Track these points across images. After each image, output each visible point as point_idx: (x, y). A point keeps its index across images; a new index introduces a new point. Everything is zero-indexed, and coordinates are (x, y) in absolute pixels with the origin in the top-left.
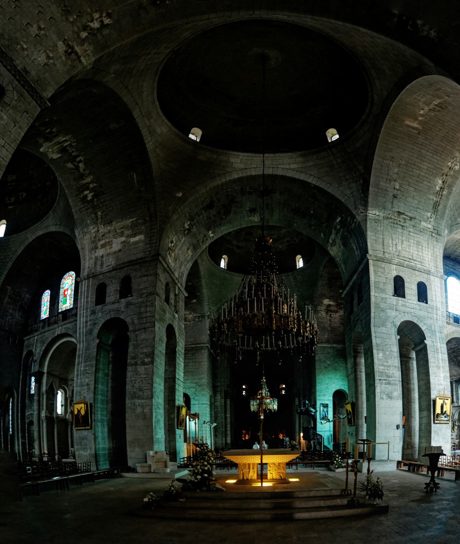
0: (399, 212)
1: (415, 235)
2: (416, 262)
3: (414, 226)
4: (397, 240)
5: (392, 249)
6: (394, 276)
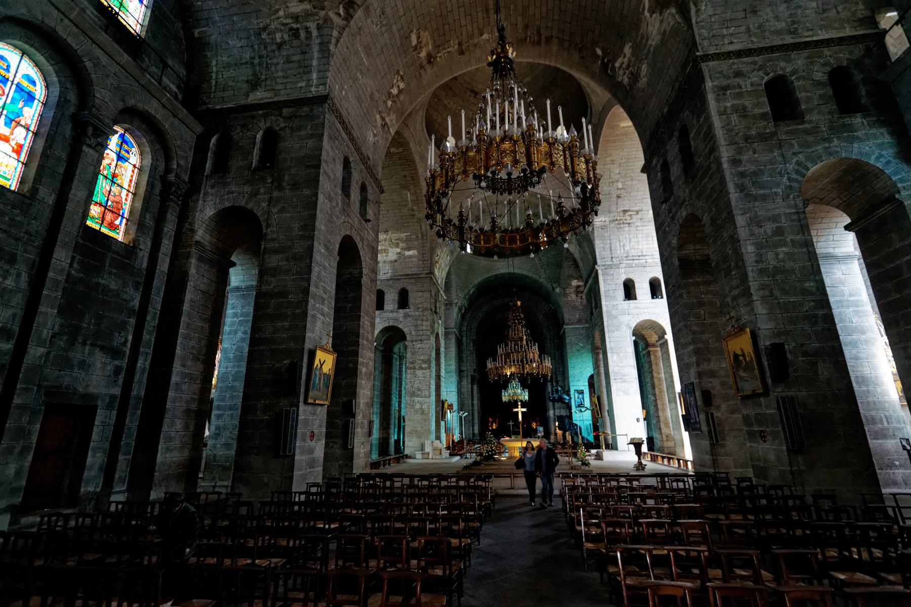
1: (644, 228)
2: (646, 257)
3: (641, 219)
4: (624, 241)
5: (619, 252)
6: (623, 280)
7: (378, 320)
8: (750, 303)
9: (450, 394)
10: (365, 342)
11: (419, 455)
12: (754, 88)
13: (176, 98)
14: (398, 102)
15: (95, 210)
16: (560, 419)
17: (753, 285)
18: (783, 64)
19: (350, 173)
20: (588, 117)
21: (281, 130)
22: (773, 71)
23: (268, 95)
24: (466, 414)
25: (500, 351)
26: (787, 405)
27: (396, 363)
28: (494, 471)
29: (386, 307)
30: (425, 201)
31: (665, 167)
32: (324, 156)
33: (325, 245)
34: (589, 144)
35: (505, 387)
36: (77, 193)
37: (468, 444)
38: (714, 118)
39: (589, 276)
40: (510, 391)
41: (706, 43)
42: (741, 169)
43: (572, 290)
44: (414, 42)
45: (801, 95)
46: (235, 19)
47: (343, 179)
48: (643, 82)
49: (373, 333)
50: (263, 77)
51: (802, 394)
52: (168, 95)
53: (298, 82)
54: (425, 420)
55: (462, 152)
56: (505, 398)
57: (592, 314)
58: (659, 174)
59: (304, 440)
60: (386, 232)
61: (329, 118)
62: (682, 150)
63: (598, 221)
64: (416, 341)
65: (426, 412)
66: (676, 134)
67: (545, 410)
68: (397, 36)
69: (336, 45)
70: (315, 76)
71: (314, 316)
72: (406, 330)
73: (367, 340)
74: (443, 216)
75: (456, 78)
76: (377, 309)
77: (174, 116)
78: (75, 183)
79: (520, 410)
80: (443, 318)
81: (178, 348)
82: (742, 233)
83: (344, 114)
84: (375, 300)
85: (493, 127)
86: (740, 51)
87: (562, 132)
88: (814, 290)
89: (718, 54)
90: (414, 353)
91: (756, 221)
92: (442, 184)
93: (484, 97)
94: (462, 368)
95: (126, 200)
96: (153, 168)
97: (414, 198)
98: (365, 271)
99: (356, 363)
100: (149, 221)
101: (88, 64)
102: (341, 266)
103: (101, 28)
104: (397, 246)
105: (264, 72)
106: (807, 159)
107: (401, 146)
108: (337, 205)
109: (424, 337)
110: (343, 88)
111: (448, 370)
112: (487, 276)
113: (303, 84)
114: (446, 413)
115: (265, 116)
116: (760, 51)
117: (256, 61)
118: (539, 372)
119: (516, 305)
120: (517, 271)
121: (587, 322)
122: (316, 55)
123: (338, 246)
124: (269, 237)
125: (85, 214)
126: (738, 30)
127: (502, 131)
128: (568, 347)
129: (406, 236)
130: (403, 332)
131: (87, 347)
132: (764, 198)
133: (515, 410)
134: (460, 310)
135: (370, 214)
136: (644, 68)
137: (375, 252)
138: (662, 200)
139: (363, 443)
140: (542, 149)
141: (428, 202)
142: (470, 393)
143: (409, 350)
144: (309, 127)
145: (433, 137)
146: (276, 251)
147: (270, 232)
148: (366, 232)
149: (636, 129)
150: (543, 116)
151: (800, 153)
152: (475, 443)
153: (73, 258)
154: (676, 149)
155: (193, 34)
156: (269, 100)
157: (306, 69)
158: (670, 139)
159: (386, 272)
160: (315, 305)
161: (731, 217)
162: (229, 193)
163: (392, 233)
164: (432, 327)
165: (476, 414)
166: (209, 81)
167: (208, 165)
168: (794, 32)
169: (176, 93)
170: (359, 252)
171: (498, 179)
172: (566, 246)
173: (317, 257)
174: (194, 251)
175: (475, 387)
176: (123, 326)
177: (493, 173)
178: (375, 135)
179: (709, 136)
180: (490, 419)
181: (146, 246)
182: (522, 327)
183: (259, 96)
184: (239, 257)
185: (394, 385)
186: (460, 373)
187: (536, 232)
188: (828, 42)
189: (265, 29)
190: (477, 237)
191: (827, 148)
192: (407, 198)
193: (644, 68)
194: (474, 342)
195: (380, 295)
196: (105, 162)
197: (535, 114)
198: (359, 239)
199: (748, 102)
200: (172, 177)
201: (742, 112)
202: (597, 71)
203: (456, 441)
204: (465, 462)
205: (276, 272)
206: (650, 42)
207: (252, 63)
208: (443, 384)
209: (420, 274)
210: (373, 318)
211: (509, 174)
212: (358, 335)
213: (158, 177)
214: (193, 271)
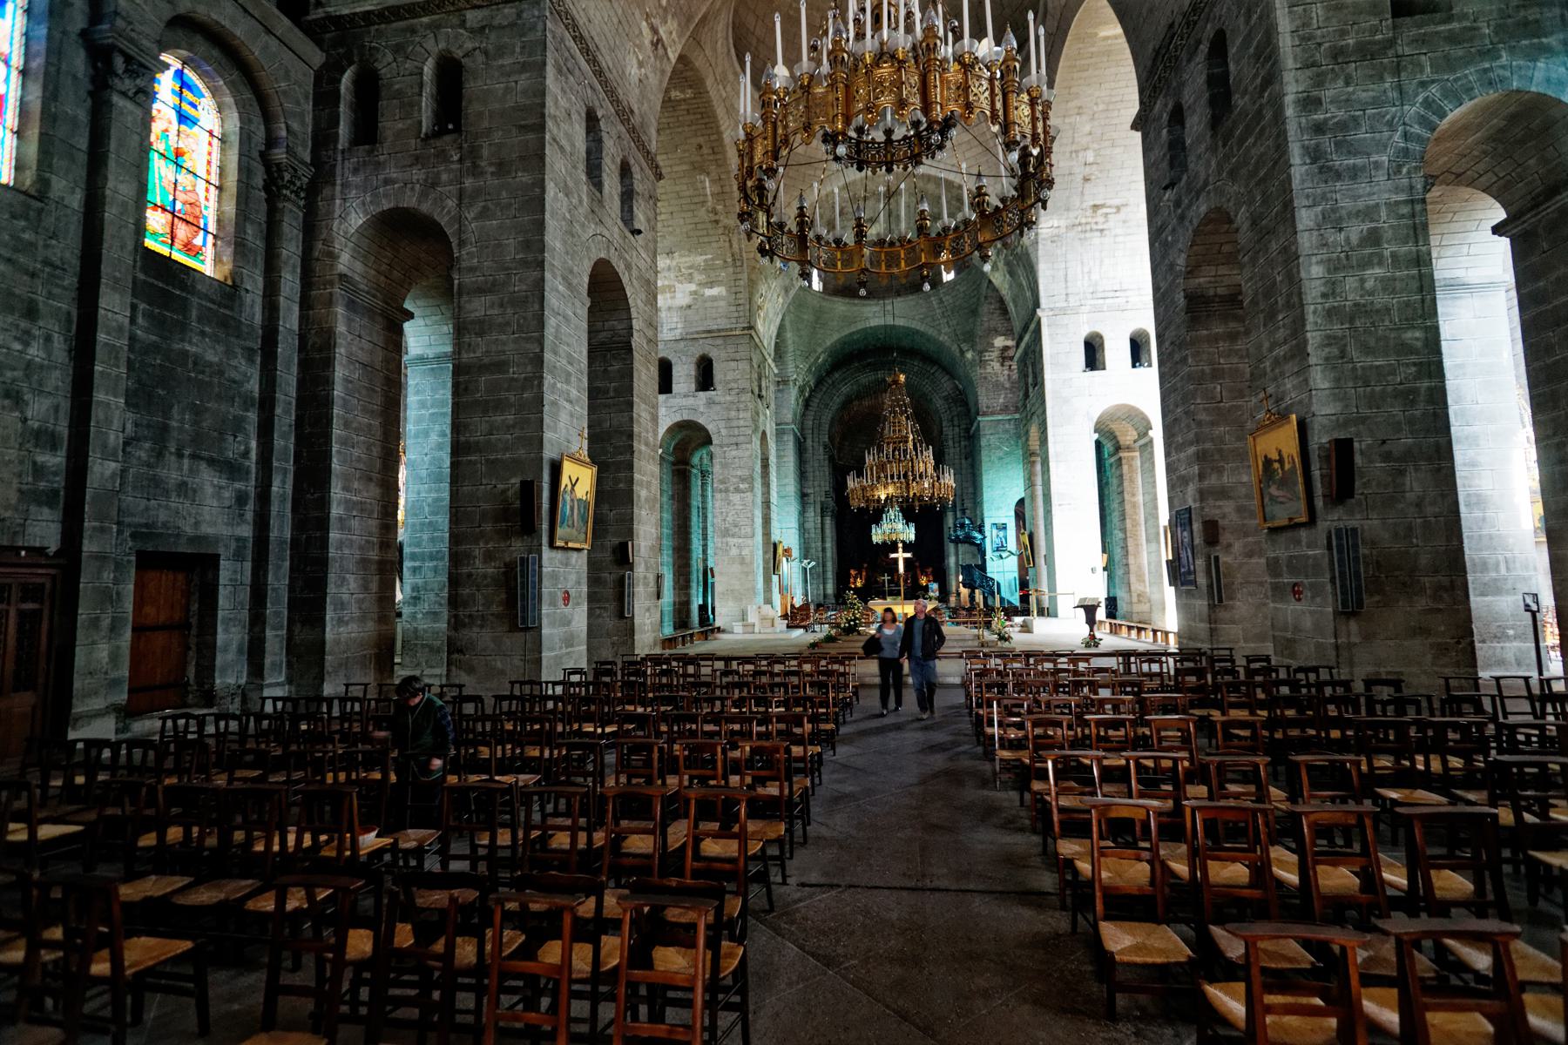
0: (1095, 206)
7: (662, 411)
8: (1304, 369)
9: (787, 531)
10: (643, 448)
11: (738, 628)
15: (156, 221)
16: (967, 570)
17: (1313, 338)
19: (600, 141)
21: (466, 55)
24: (813, 563)
25: (869, 459)
26: (1344, 542)
27: (696, 484)
29: (675, 387)
30: (735, 187)
31: (1178, 116)
32: (550, 108)
33: (564, 278)
36: (117, 186)
37: (816, 611)
38: (1278, 12)
39: (1025, 329)
40: (886, 526)
42: (1319, 116)
43: (996, 354)
47: (589, 152)
49: (655, 433)
51: (1370, 524)
54: (747, 574)
56: (877, 536)
57: (1026, 395)
58: (1165, 131)
59: (553, 604)
60: (670, 253)
62: (1211, 81)
63: (1048, 224)
64: (728, 445)
65: (747, 561)
66: (1204, 48)
67: (941, 557)
71: (554, 403)
72: (710, 428)
73: (647, 444)
76: (661, 392)
77: (269, 31)
79: (901, 556)
80: (773, 406)
81: (334, 460)
82: (1306, 241)
83: (581, 20)
88: (1419, 344)
90: (724, 466)
91: (1332, 219)
94: (805, 491)
95: (207, 199)
96: (245, 138)
97: (717, 189)
98: (636, 324)
99: (631, 481)
104: (690, 279)
107: (690, 87)
108: (581, 201)
109: (742, 439)
112: (847, 332)
119: (896, 382)
120: (900, 322)
121: (1017, 410)
123: (586, 280)
124: (464, 264)
125: (140, 229)
128: (984, 453)
129: (706, 261)
130: (706, 431)
131: (186, 461)
132: (1354, 173)
133: (893, 556)
134: (801, 390)
135: (640, 221)
138: (1167, 182)
139: (648, 610)
142: (819, 531)
146: (480, 291)
147: (467, 255)
148: (635, 253)
151: (1433, 82)
152: (828, 609)
153: (134, 307)
159: (673, 326)
160: (555, 384)
161: (1288, 209)
162: (387, 182)
163: (681, 256)
164: (755, 421)
165: (829, 565)
167: (344, 130)
170: (624, 289)
171: (868, 143)
173: (552, 300)
175: (828, 521)
176: (238, 426)
177: (860, 130)
178: (641, 65)
180: (853, 572)
181: (254, 284)
182: (907, 418)
184: (418, 303)
186: (803, 496)
191: (1485, 71)
192: (704, 188)
194: (825, 447)
195: (665, 369)
196: (156, 128)
198: (622, 266)
200: (280, 154)
204: (811, 638)
208: (774, 516)
209: (731, 330)
210: (655, 407)
211: (889, 132)
212: (631, 436)
213: (255, 154)
214: (341, 328)
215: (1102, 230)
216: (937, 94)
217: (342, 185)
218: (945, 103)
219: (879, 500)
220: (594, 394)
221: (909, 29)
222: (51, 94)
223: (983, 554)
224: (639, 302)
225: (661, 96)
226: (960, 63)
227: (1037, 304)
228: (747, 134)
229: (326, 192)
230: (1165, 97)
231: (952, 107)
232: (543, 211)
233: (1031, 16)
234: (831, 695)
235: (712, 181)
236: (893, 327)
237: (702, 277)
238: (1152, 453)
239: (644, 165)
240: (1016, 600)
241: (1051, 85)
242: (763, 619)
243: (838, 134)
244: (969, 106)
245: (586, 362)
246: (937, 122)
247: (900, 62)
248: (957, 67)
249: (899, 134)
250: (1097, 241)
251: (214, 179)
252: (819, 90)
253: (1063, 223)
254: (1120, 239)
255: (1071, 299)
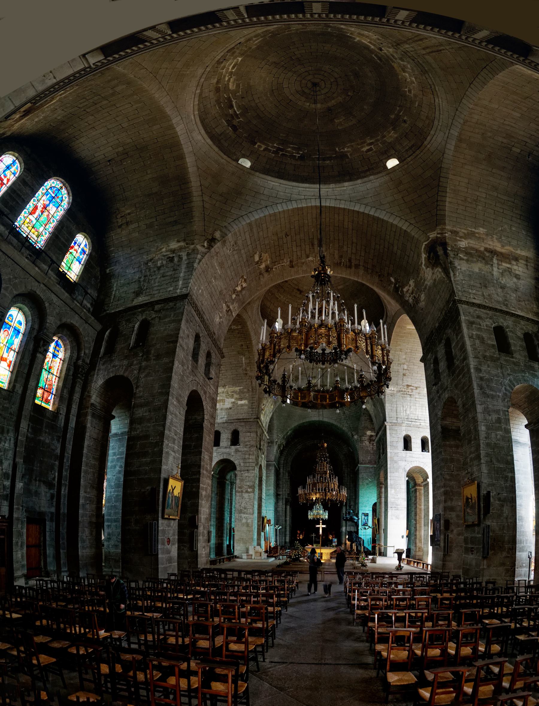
7: (215, 454)
9: (269, 512)
12: (488, 328)
13: (89, 310)
14: (240, 295)
15: (39, 392)
16: (350, 533)
18: (502, 320)
19: (200, 344)
20: (384, 319)
21: (152, 319)
22: (497, 322)
23: (146, 298)
24: (280, 527)
25: (309, 481)
27: (228, 491)
28: (300, 569)
30: (256, 366)
34: (384, 337)
35: (311, 508)
36: (32, 383)
37: (281, 549)
39: (380, 429)
40: (315, 512)
41: (460, 294)
44: (257, 258)
45: (511, 341)
46: (133, 258)
47: (194, 349)
48: (422, 304)
49: (211, 464)
50: (145, 288)
52: (85, 310)
53: (169, 288)
55: (287, 332)
56: (311, 515)
57: (379, 458)
60: (224, 386)
61: (188, 308)
62: (446, 353)
63: (390, 390)
67: (340, 527)
68: (244, 256)
69: (199, 263)
70: (181, 282)
73: (207, 471)
74: (270, 377)
75: (286, 281)
76: (215, 446)
77: (86, 322)
78: (32, 376)
79: (321, 526)
80: (265, 453)
83: (199, 304)
84: (213, 439)
85: (313, 316)
86: (479, 305)
87: (365, 324)
89: (468, 302)
92: (270, 355)
93: (307, 297)
96: (71, 357)
97: (248, 361)
98: (206, 417)
99: (198, 487)
100: (66, 394)
101: (47, 305)
102: (188, 413)
103: (57, 283)
105: (146, 284)
106: (514, 379)
107: (240, 325)
108: (188, 368)
110: (200, 289)
111: (268, 494)
112: (301, 422)
113: (172, 289)
114: (265, 526)
115: (142, 312)
116: (491, 309)
117: (142, 279)
118: (337, 499)
119: (323, 446)
120: (326, 420)
121: (375, 463)
122: (183, 270)
123: (186, 399)
124: (138, 395)
125: (35, 396)
126: (477, 293)
127: (320, 321)
128: (360, 481)
130: (234, 464)
133: (317, 526)
134: (279, 447)
135: (213, 374)
136: (423, 297)
137: (214, 402)
138: (434, 383)
140: (349, 336)
141: (259, 367)
142: (284, 512)
143: (238, 478)
144: (172, 316)
145: (266, 321)
146: (142, 406)
147: (139, 391)
149: (418, 332)
150: (351, 313)
152: (286, 549)
153: (29, 425)
154: (443, 351)
155: (106, 271)
156: (148, 301)
157: (175, 279)
158: (439, 344)
159: (223, 417)
162: (113, 366)
164: (257, 460)
166: (110, 297)
167: (102, 350)
168: (506, 305)
169: (89, 309)
171: (315, 353)
172: (364, 407)
173: (171, 408)
174: (89, 410)
175: (288, 507)
176: (52, 468)
177: (311, 348)
179: (463, 348)
180: (298, 532)
181: (63, 412)
182: (327, 463)
183: (141, 299)
184: (118, 411)
185: (226, 504)
186: (277, 496)
187: (342, 392)
188: (522, 318)
189: (151, 260)
190: (295, 393)
191: (523, 376)
193: (423, 297)
194: (289, 473)
195: (217, 435)
196: (46, 361)
197: (346, 312)
198: (202, 392)
199: (485, 335)
200: (80, 362)
201: (482, 340)
202: (391, 290)
203: (272, 547)
204: (278, 562)
205: (141, 420)
206: (426, 282)
207: (139, 281)
210: (211, 453)
211: (324, 350)
212: (199, 466)
213: (72, 364)
214: (89, 425)
215: (411, 395)
216: (344, 341)
217: (98, 370)
218: (347, 344)
219: (312, 500)
220: (185, 448)
221: (333, 317)
222: (22, 358)
223: (358, 526)
224: (208, 407)
225: (227, 328)
226: (353, 332)
227: (385, 420)
228: (262, 347)
229: (92, 373)
230: (432, 353)
231: (350, 347)
232: (172, 373)
233: (381, 321)
234: (286, 586)
235: (246, 359)
236: (323, 422)
237: (238, 396)
238: (428, 488)
239: (217, 353)
240: (370, 548)
241: (389, 345)
242: (256, 552)
243: (302, 350)
244: (357, 347)
245: (182, 434)
246: (344, 351)
247: (329, 328)
248: (352, 333)
249: (328, 351)
250: (409, 399)
251: (58, 375)
252: (295, 334)
253: (395, 389)
254: (417, 399)
255: (398, 419)
